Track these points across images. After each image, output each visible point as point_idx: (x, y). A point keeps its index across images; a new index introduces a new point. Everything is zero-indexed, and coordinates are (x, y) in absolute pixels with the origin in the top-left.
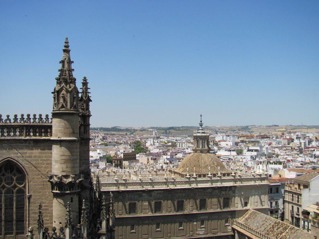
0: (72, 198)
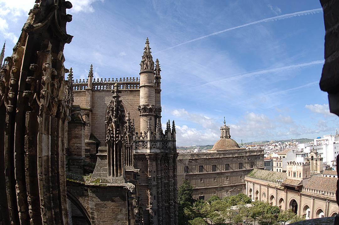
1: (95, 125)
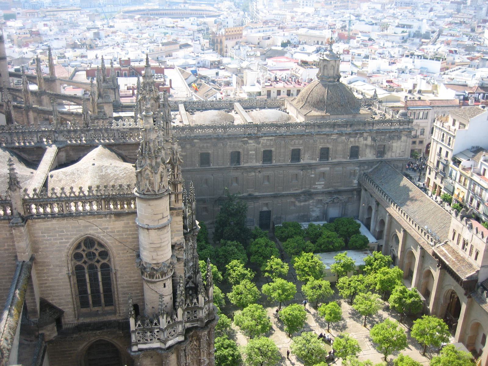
0: (165, 285)
1: (46, 283)
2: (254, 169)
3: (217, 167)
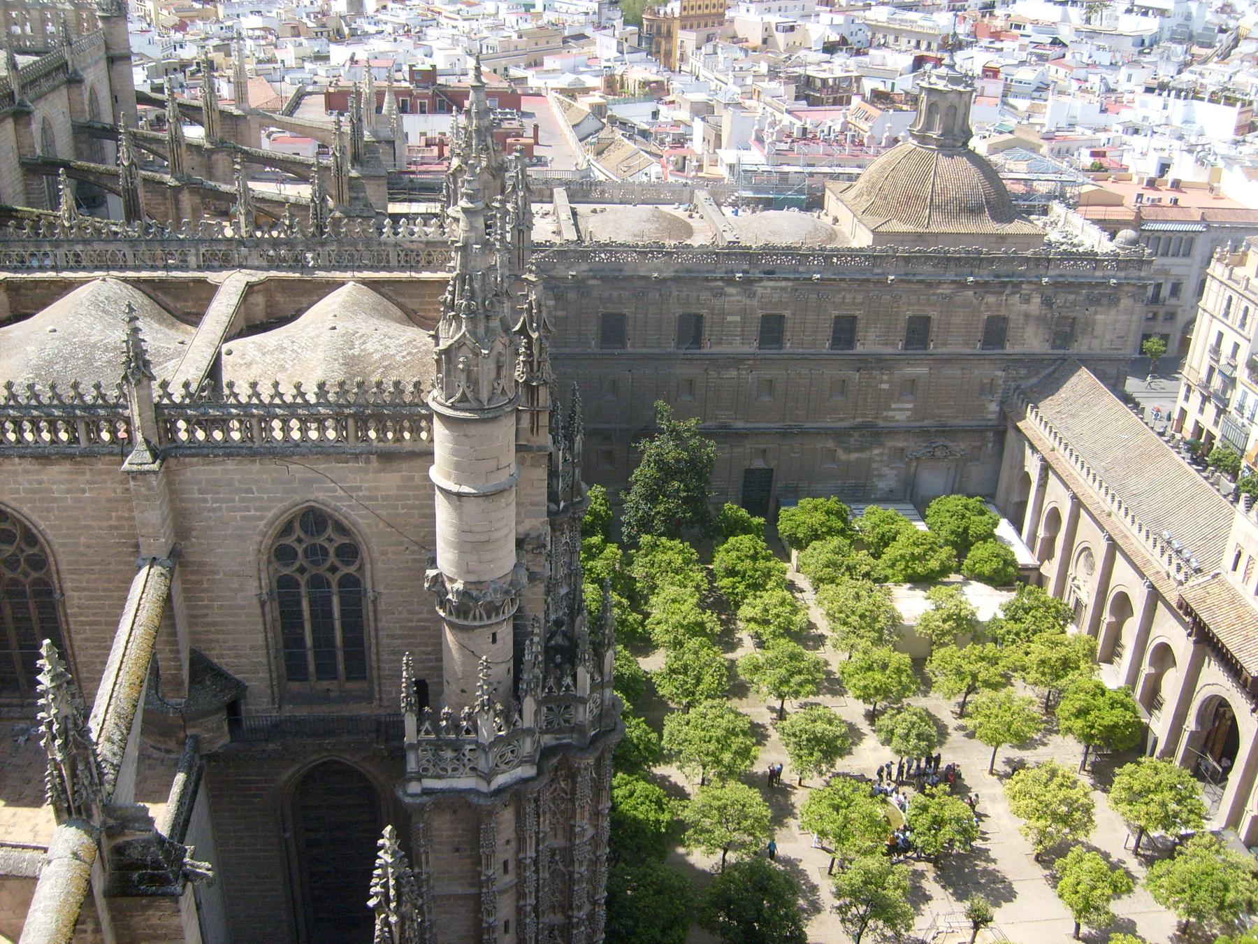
0: (494, 635)
1: (206, 615)
2: (736, 361)
3: (644, 350)
